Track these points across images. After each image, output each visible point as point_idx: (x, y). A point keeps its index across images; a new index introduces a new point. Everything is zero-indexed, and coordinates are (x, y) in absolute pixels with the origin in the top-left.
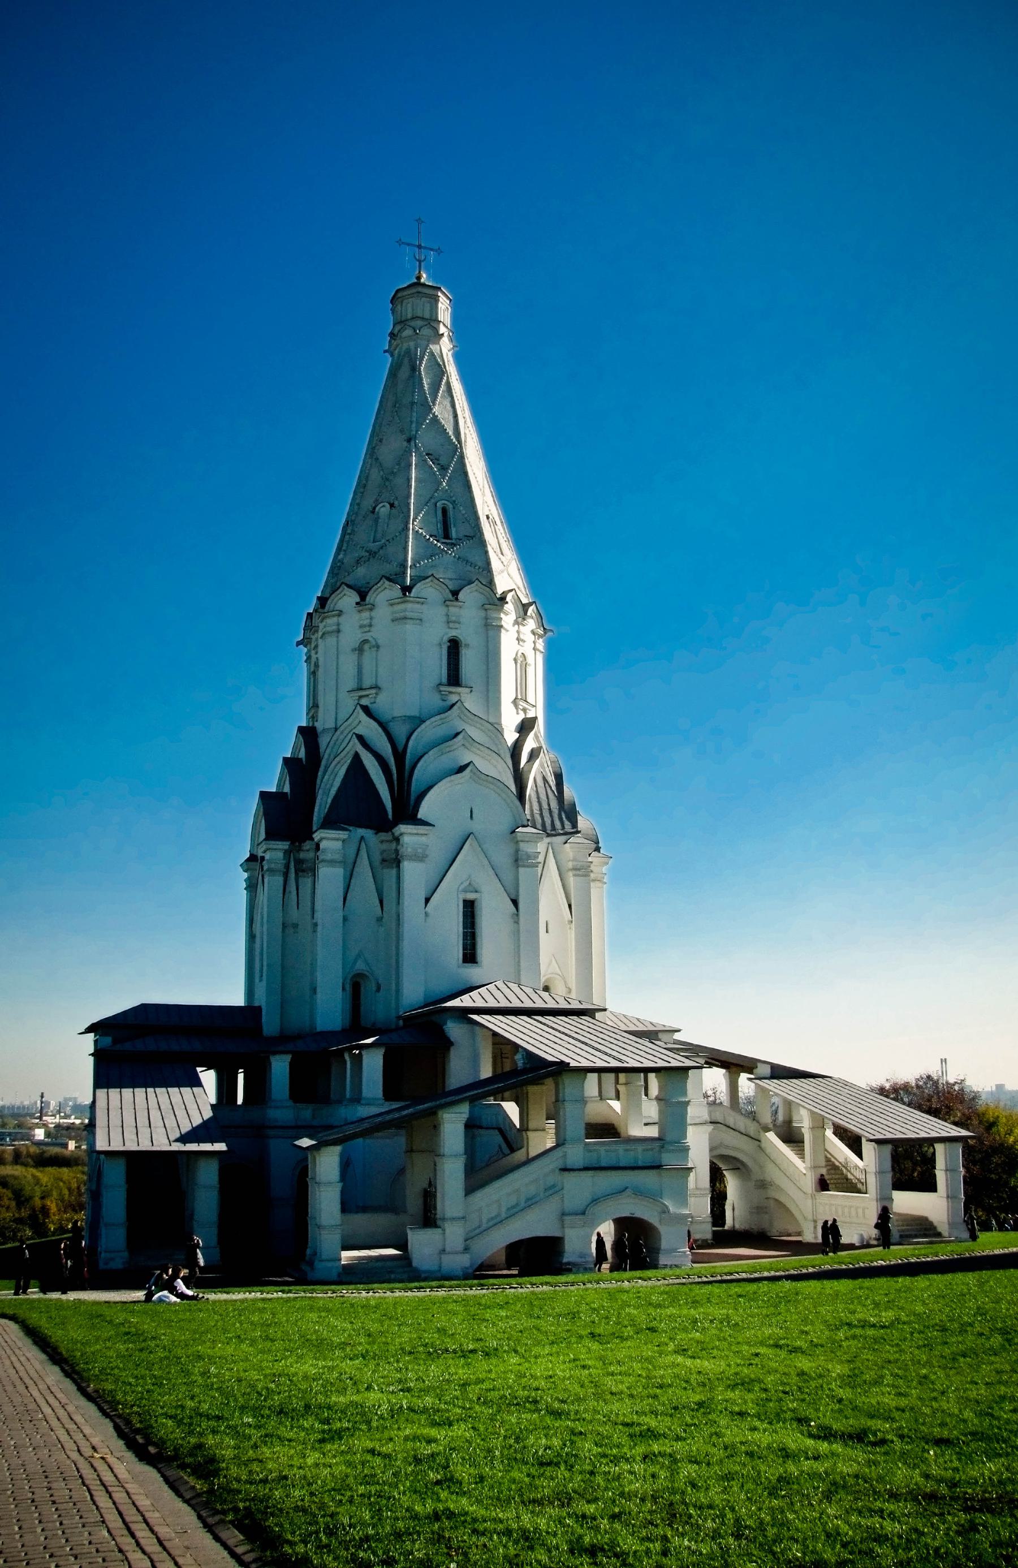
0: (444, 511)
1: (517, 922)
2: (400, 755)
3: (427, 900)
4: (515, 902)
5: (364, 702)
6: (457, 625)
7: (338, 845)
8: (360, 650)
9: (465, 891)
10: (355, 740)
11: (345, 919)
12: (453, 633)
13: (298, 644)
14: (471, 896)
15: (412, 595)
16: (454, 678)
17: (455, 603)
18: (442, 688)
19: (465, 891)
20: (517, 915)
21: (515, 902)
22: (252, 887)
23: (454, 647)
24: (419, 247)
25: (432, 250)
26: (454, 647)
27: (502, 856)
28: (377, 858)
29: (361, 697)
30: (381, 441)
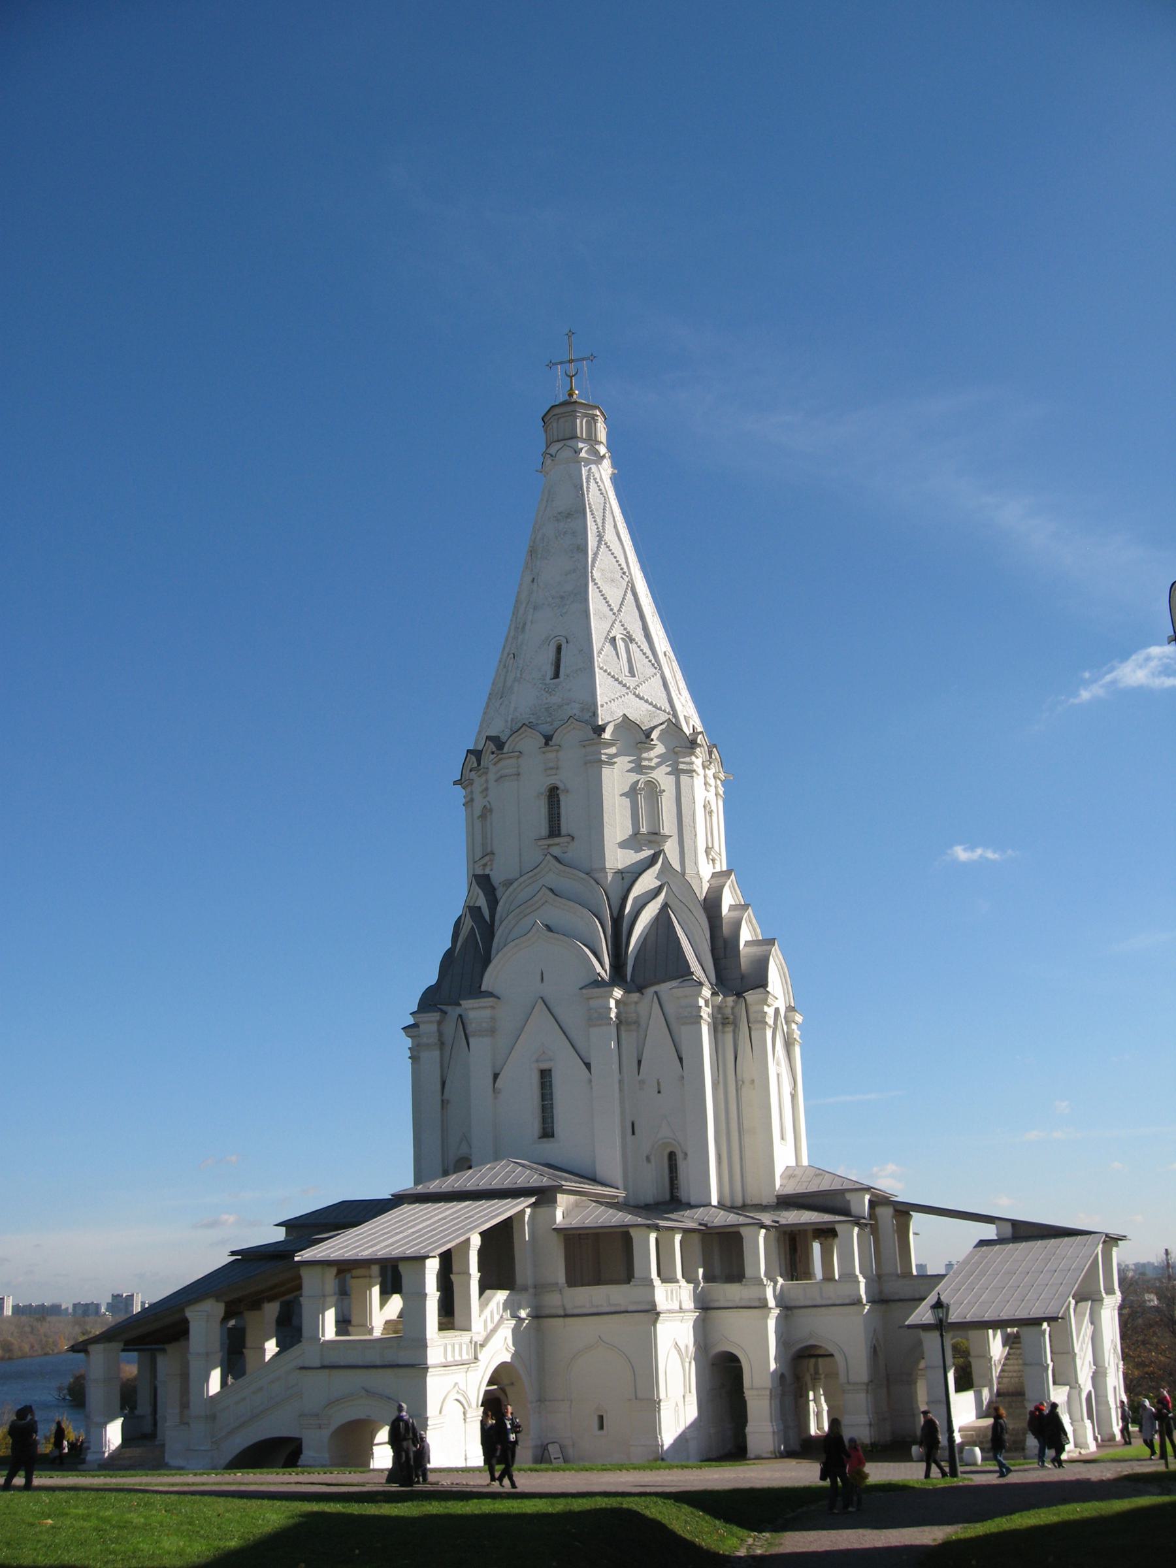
0: (559, 649)
3: (496, 1076)
4: (588, 1066)
6: (554, 771)
7: (434, 1027)
8: (483, 817)
11: (444, 1103)
12: (552, 780)
14: (545, 1066)
15: (505, 750)
16: (554, 830)
17: (548, 748)
18: (540, 843)
21: (588, 1066)
23: (553, 795)
25: (583, 359)
26: (553, 795)
29: (485, 865)
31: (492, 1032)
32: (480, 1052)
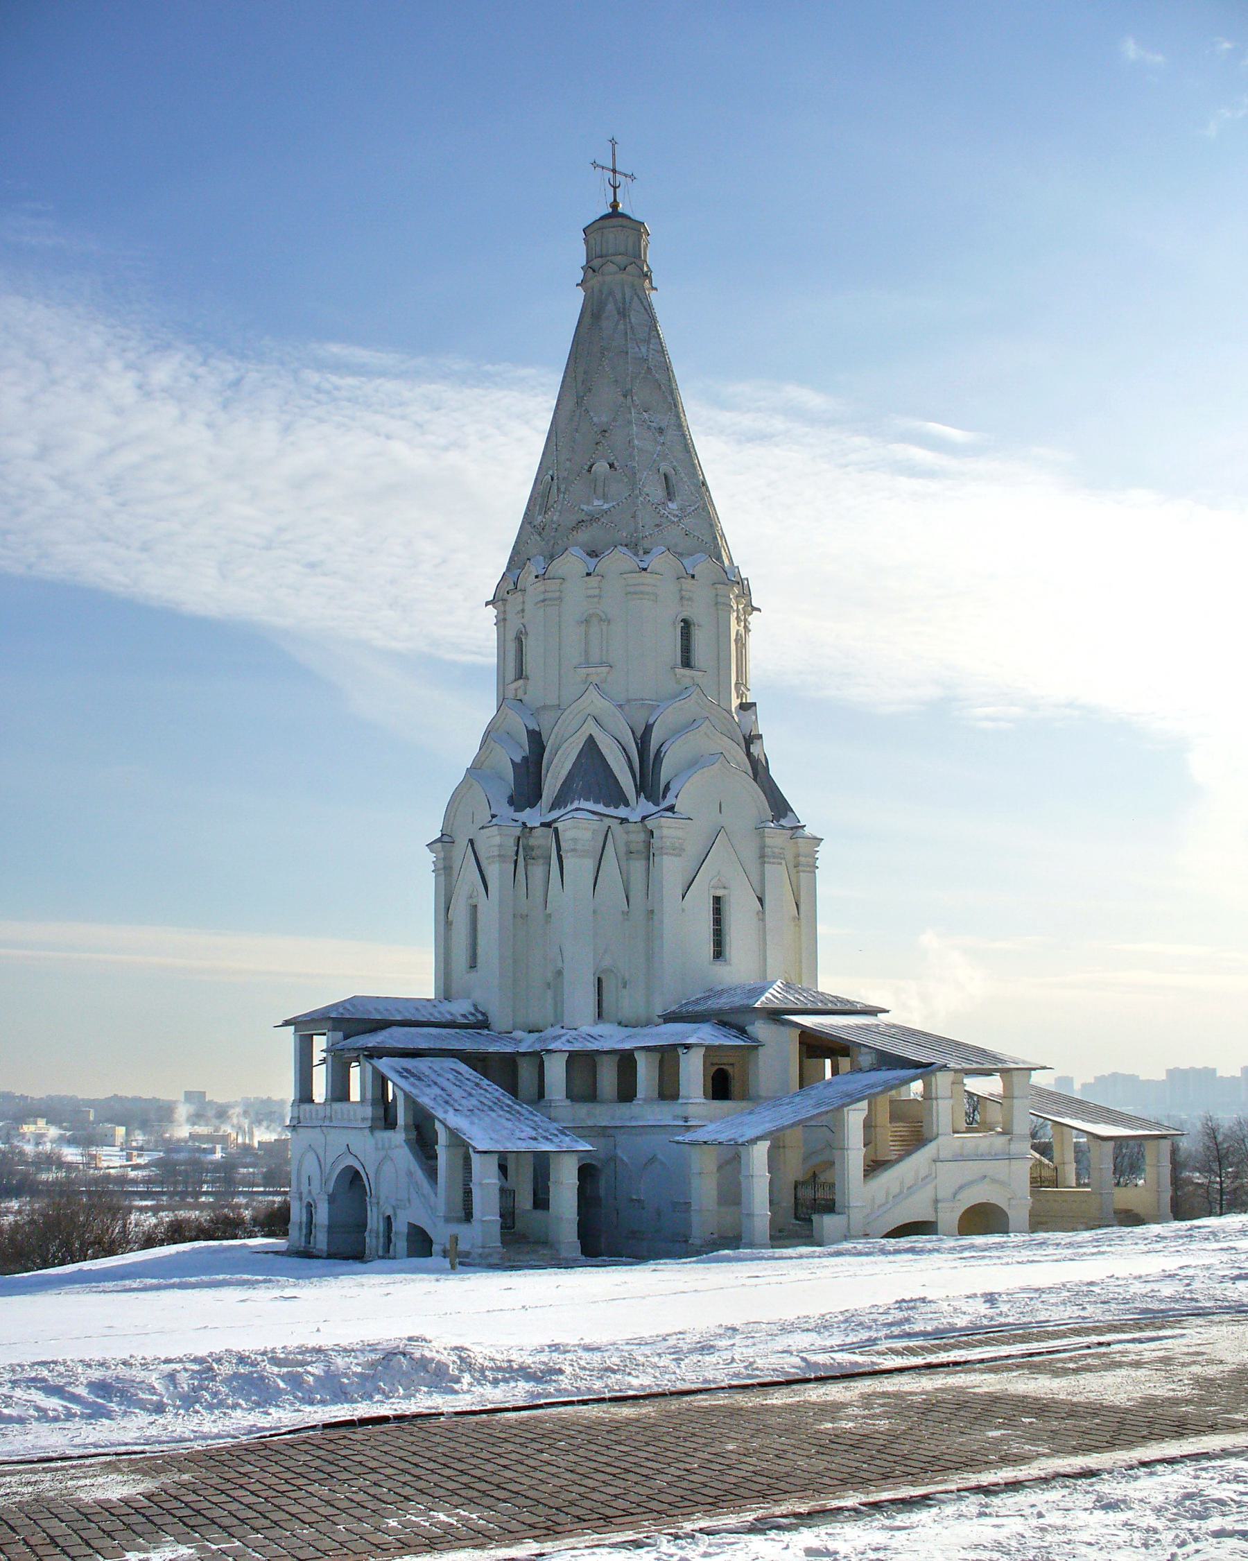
1: (763, 920)
2: (643, 741)
4: (760, 900)
5: (595, 679)
8: (587, 621)
9: (716, 888)
10: (591, 722)
11: (594, 912)
13: (487, 604)
14: (719, 893)
19: (716, 888)
20: (763, 913)
22: (445, 870)
24: (614, 171)
27: (749, 852)
28: (622, 849)
30: (590, 390)
31: (678, 851)
32: (671, 869)
